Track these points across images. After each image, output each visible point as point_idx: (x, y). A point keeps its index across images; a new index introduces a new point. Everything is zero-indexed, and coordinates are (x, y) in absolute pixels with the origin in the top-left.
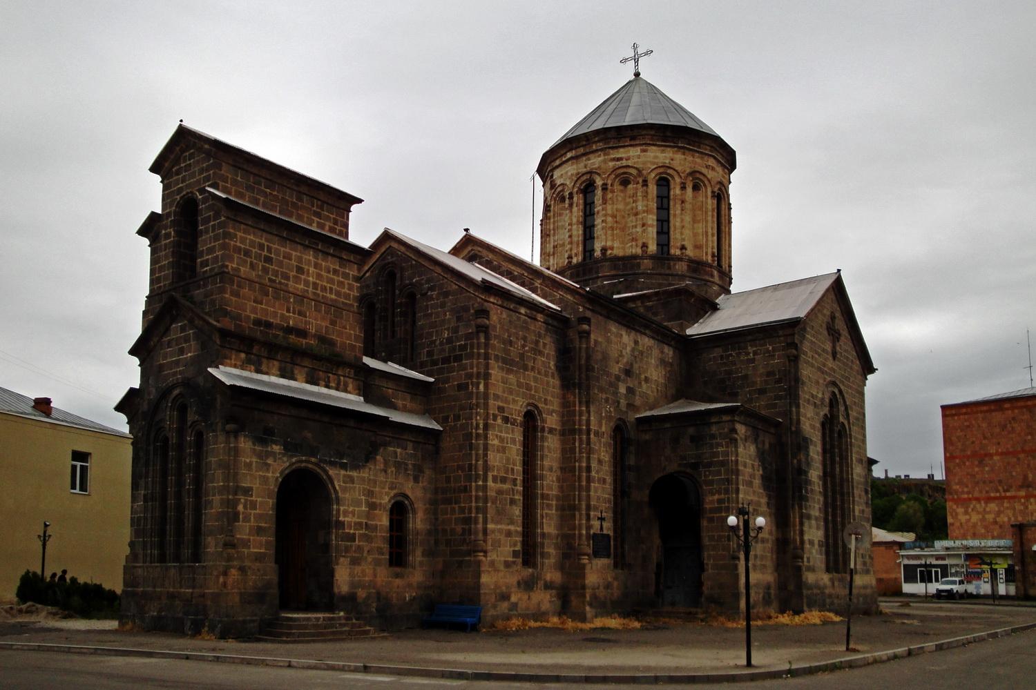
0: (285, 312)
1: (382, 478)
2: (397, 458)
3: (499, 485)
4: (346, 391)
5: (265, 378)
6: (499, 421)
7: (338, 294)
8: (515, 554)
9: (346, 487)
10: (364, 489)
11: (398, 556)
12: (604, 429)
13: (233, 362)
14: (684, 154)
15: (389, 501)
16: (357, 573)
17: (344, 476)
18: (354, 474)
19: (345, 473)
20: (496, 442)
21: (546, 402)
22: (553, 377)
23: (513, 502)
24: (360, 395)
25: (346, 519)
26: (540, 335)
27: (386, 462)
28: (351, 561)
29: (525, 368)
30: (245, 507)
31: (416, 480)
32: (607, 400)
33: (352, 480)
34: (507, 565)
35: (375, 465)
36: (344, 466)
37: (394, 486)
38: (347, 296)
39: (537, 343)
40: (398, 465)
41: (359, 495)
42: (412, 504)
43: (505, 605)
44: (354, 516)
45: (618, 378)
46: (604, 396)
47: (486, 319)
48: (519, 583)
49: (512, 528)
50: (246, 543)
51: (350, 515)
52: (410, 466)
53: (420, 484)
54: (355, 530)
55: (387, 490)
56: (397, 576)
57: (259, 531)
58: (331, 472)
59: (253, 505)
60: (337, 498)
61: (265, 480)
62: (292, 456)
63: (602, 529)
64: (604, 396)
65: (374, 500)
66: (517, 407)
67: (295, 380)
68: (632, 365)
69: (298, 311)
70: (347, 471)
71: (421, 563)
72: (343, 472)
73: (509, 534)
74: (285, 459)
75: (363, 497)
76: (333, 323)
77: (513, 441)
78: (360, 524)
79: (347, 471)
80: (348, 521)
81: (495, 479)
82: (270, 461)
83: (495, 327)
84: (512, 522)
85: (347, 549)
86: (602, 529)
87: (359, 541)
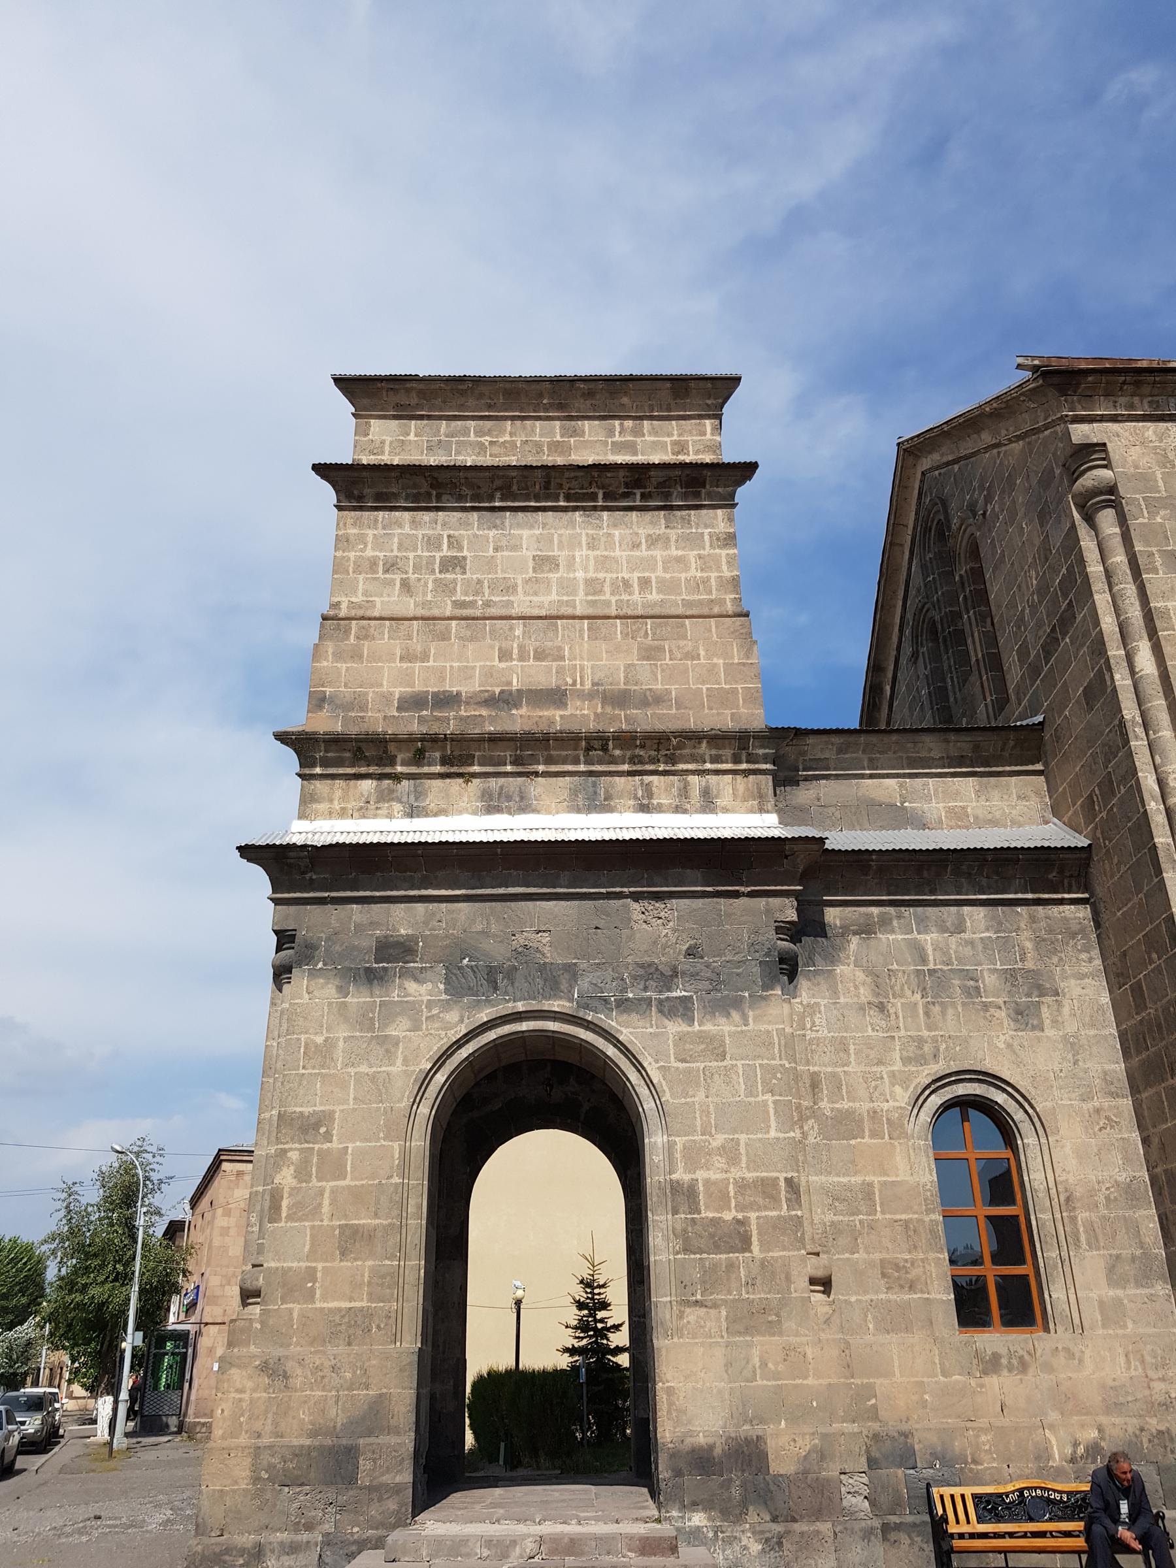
0: (496, 663)
1: (871, 1028)
2: (924, 961)
9: (689, 1071)
10: (769, 1071)
11: (999, 1287)
13: (336, 806)
15: (918, 1101)
16: (764, 1364)
17: (681, 1038)
18: (723, 1027)
19: (684, 1028)
24: (761, 810)
25: (701, 1175)
27: (879, 980)
28: (732, 1320)
30: (302, 1173)
31: (1024, 1016)
35: (835, 993)
36: (681, 1009)
37: (927, 1048)
40: (934, 984)
41: (750, 1093)
42: (1023, 1100)
44: (734, 1160)
47: (1105, 467)
50: (298, 1286)
51: (719, 1162)
52: (990, 980)
53: (1050, 1032)
54: (740, 1207)
55: (898, 1066)
56: (992, 1365)
57: (351, 1240)
58: (625, 1035)
59: (334, 1166)
60: (661, 1109)
61: (378, 1085)
62: (477, 1005)
65: (845, 1105)
67: (535, 811)
69: (536, 651)
70: (691, 1021)
71: (1112, 1313)
72: (675, 1027)
74: (453, 1016)
75: (768, 1097)
78: (766, 1188)
79: (691, 1021)
80: (707, 1182)
82: (392, 1031)
85: (712, 1278)
87: (765, 1246)
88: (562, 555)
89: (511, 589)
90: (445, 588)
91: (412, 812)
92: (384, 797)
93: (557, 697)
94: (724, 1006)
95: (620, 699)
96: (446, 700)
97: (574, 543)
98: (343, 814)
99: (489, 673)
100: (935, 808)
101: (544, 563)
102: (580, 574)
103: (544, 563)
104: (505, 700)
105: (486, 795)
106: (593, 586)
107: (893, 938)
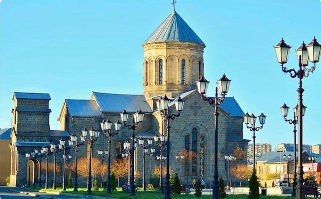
4: (45, 142)
5: (26, 142)
7: (44, 122)
14: (170, 50)
67: (33, 141)
83: (77, 125)
88: (35, 118)
89: (31, 122)
91: (25, 141)
93: (34, 132)
95: (39, 132)
96: (27, 132)
97: (36, 118)
98: (20, 141)
99: (30, 130)
101: (34, 119)
102: (37, 121)
103: (34, 119)
104: (31, 132)
105: (29, 140)
106: (38, 122)
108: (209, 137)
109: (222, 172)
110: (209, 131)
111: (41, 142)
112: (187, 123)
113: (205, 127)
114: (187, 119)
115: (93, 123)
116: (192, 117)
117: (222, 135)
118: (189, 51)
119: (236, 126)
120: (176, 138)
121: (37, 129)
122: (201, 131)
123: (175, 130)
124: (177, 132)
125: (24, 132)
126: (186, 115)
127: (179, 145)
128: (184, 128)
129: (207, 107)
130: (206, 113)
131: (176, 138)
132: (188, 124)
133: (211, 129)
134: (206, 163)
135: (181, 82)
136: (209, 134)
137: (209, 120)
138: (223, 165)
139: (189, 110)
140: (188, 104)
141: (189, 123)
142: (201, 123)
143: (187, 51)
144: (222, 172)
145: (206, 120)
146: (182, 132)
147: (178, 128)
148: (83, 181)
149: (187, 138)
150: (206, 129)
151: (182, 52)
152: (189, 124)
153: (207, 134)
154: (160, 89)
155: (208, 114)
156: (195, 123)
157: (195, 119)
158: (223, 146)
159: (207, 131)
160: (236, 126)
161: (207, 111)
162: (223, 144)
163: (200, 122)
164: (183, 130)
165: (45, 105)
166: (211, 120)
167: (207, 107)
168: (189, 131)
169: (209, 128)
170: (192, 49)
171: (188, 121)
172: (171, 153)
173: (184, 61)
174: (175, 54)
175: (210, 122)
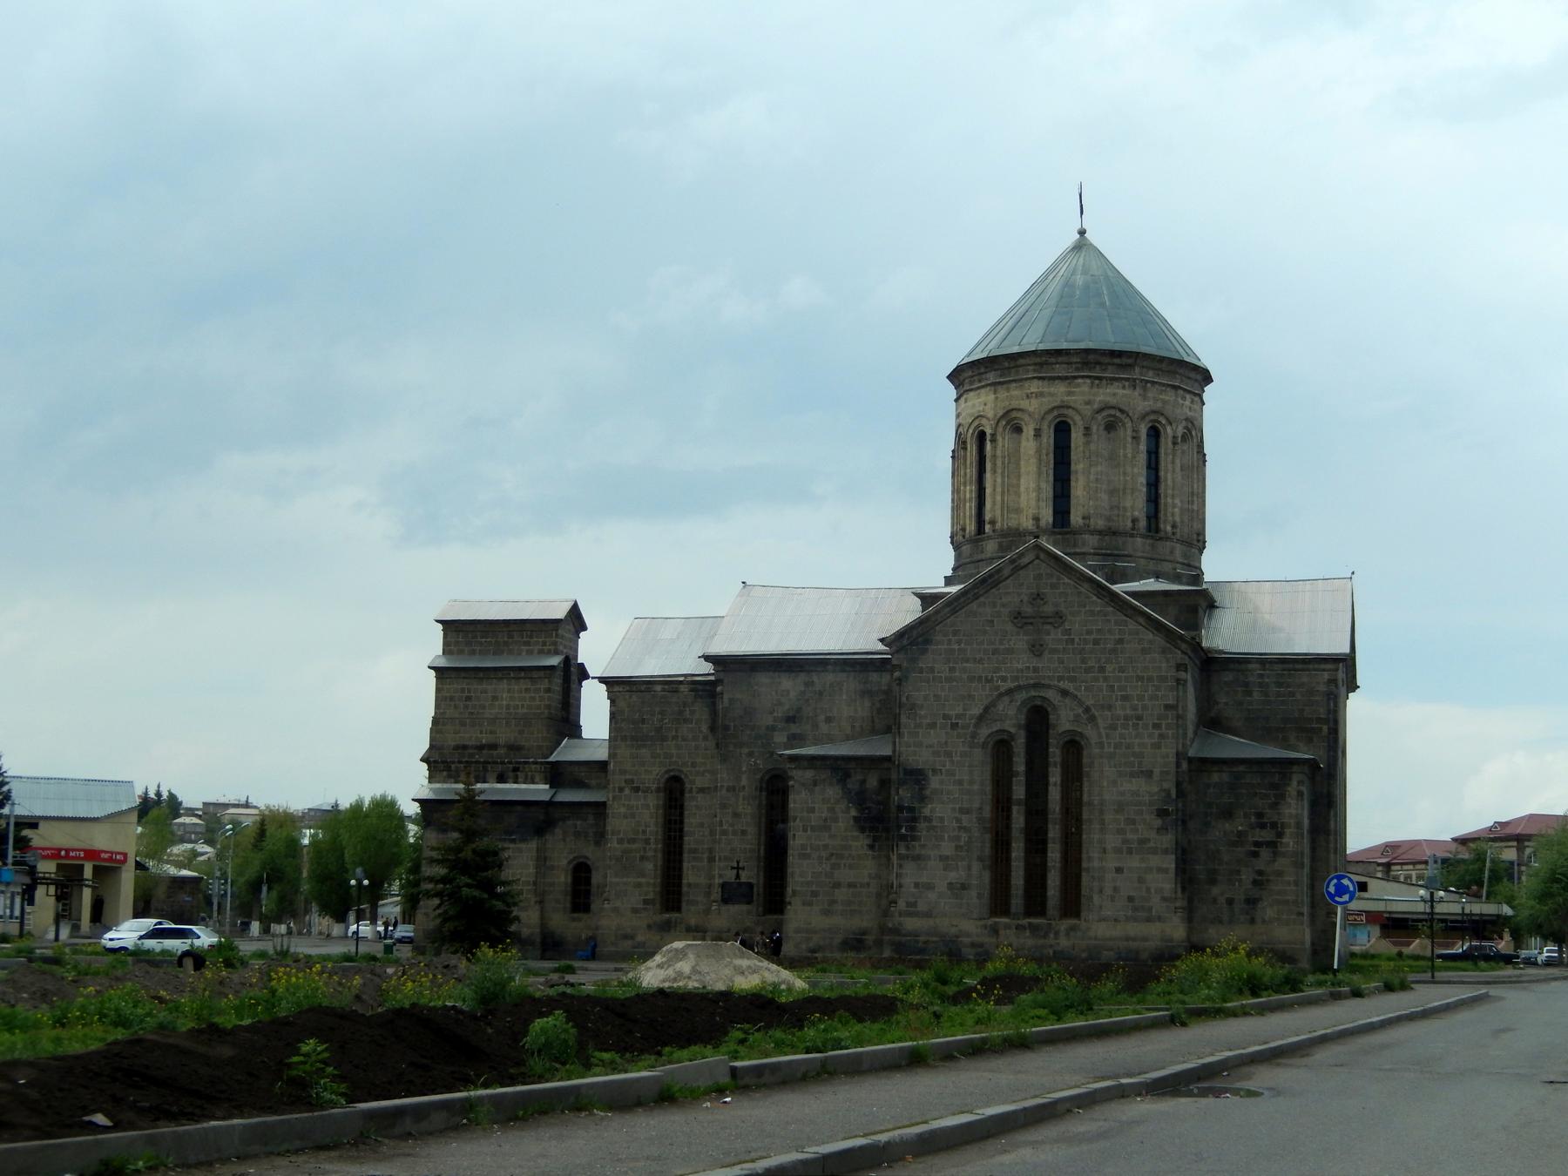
3: (626, 845)
6: (627, 791)
8: (646, 902)
12: (744, 782)
14: (1008, 390)
18: (523, 846)
20: (623, 810)
21: (694, 765)
22: (705, 738)
23: (642, 858)
26: (685, 705)
29: (664, 739)
31: (597, 843)
32: (751, 754)
33: (520, 850)
34: (635, 911)
36: (513, 841)
38: (539, 707)
39: (681, 713)
40: (577, 834)
43: (630, 942)
45: (772, 729)
46: (745, 750)
48: (649, 927)
49: (643, 880)
56: (574, 920)
63: (738, 876)
64: (745, 750)
66: (653, 774)
68: (799, 710)
73: (639, 885)
76: (521, 732)
77: (648, 806)
81: (620, 841)
84: (643, 876)
86: (738, 876)
90: (466, 707)
92: (449, 777)
93: (493, 747)
94: (523, 840)
95: (514, 748)
96: (465, 747)
100: (593, 782)
103: (495, 698)
104: (481, 748)
106: (508, 707)
107: (569, 823)
108: (1101, 745)
109: (1164, 899)
110: (1100, 721)
111: (515, 786)
112: (997, 688)
113: (1080, 703)
114: (997, 670)
115: (685, 705)
116: (1023, 661)
117: (1161, 736)
118: (1086, 389)
119: (1299, 697)
120: (949, 754)
121: (504, 735)
122: (1064, 720)
123: (945, 717)
124: (954, 726)
125: (457, 748)
126: (995, 652)
127: (960, 782)
128: (986, 709)
129: (1092, 613)
130: (1086, 642)
131: (949, 754)
132: (1002, 690)
133: (1110, 707)
134: (1090, 859)
135: (1047, 516)
136: (1103, 732)
137: (1102, 669)
138: (1166, 871)
139: (1009, 627)
140: (1003, 605)
141: (1012, 685)
142: (1064, 685)
143: (1078, 385)
144: (1164, 899)
145: (1088, 670)
146: (977, 725)
147: (959, 710)
148: (640, 938)
149: (1001, 747)
150: (1087, 710)
151: (1051, 394)
152: (1010, 692)
153: (1089, 731)
154: (976, 558)
155: (1096, 642)
156: (1036, 686)
157: (1036, 670)
158: (1166, 785)
159: (1092, 719)
160: (1299, 697)
161: (1089, 632)
162: (1167, 773)
163: (1060, 679)
164: (981, 719)
165: (544, 644)
166: (1109, 668)
167: (1092, 613)
168: (1011, 718)
169: (1102, 707)
170: (1100, 378)
171: (1004, 679)
172: (928, 819)
173: (1062, 430)
174: (1024, 404)
175: (1106, 679)
